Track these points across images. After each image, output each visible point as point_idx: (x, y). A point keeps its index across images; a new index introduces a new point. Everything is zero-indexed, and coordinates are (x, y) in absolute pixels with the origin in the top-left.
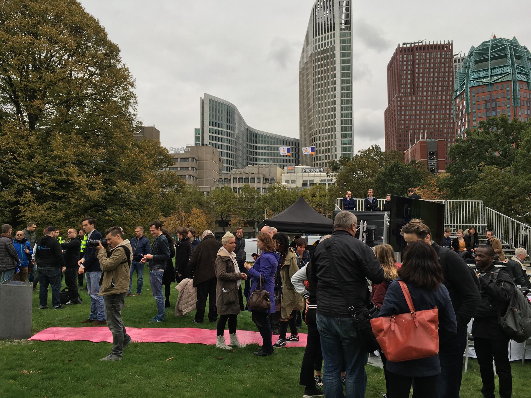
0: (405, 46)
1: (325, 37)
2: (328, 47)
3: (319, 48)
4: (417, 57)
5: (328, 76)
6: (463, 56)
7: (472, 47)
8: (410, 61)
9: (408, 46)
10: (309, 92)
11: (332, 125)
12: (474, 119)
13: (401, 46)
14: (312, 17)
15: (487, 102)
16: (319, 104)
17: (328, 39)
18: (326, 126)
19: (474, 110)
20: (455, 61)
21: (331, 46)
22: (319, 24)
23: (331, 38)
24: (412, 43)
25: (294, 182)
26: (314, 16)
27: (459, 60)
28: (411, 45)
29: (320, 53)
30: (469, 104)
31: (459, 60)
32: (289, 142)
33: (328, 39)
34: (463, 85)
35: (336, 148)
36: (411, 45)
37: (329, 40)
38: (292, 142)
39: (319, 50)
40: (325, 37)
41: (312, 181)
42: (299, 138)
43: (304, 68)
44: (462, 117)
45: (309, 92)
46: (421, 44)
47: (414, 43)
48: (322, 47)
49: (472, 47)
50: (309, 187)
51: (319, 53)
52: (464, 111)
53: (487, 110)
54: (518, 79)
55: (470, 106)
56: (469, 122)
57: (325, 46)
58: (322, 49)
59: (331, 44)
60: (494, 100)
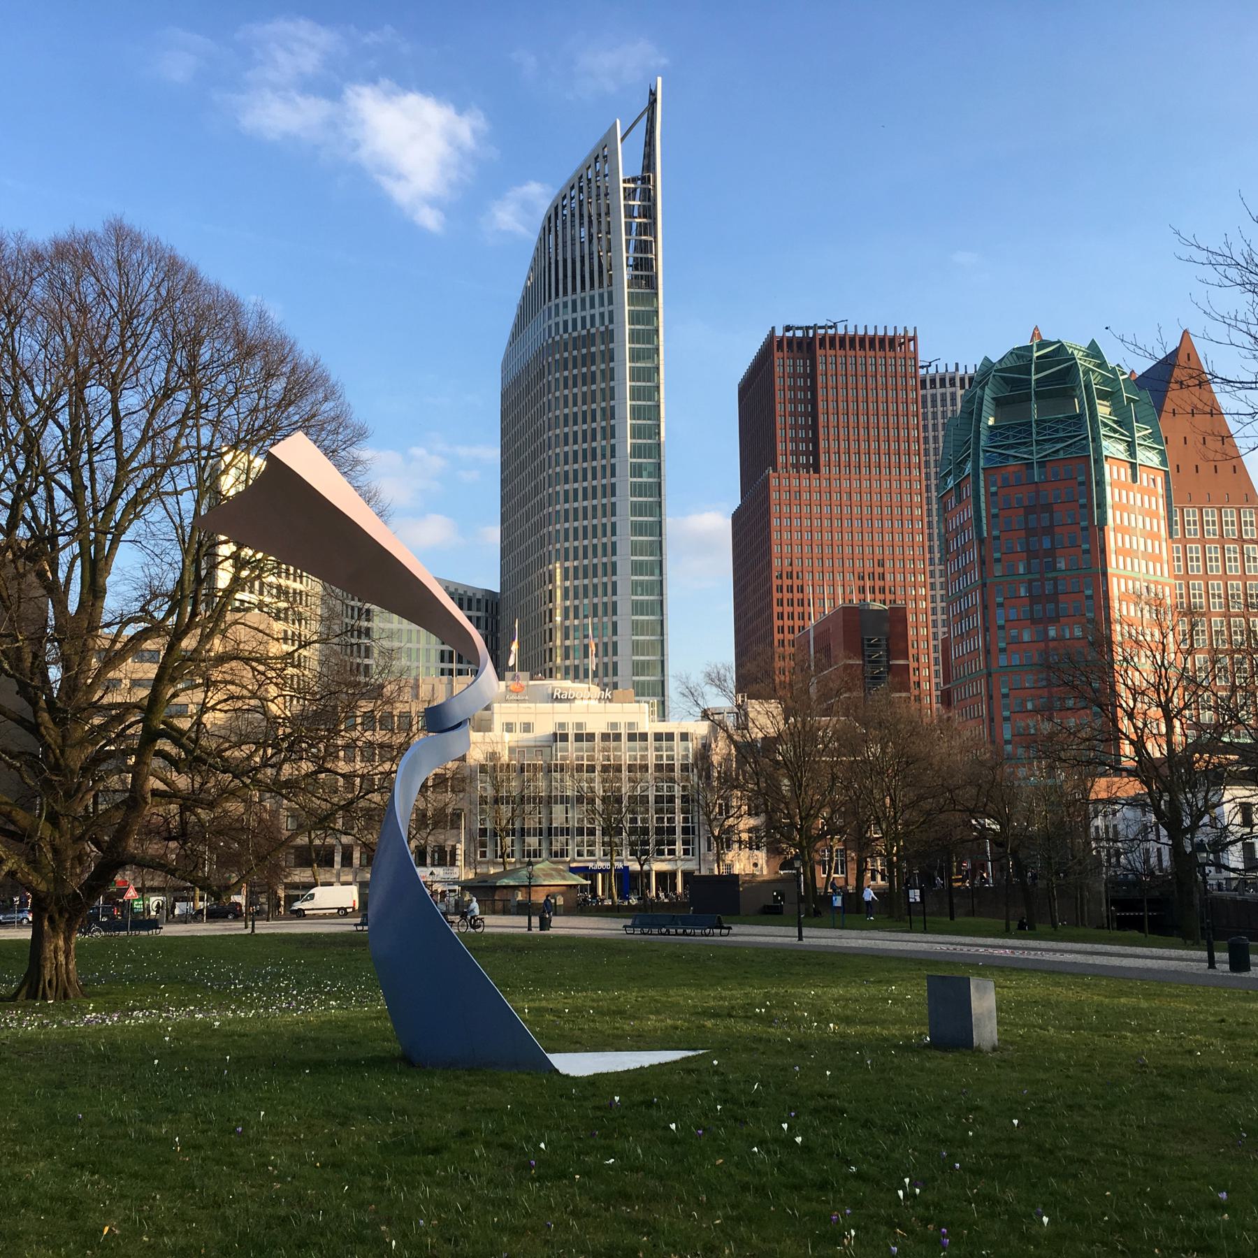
0: (790, 334)
1: (583, 300)
2: (593, 331)
3: (566, 331)
4: (821, 368)
5: (594, 411)
6: (942, 370)
7: (986, 359)
8: (804, 376)
9: (799, 334)
10: (534, 455)
11: (605, 555)
12: (997, 555)
13: (779, 333)
14: (543, 239)
15: (1029, 510)
16: (566, 492)
17: (592, 306)
18: (585, 557)
19: (996, 533)
20: (923, 382)
21: (602, 329)
22: (565, 261)
23: (602, 304)
24: (808, 328)
25: (527, 727)
26: (552, 237)
27: (933, 381)
29: (570, 347)
30: (984, 513)
31: (933, 381)
32: (470, 600)
33: (592, 306)
34: (965, 461)
35: (615, 625)
37: (597, 311)
38: (479, 601)
39: (566, 336)
40: (583, 300)
41: (579, 725)
42: (496, 589)
43: (517, 382)
44: (964, 550)
45: (534, 455)
46: (831, 332)
47: (815, 327)
48: (575, 328)
49: (986, 359)
50: (571, 744)
51: (566, 344)
52: (970, 534)
53: (1030, 532)
54: (1105, 453)
55: (984, 521)
56: (982, 562)
57: (584, 327)
58: (575, 334)
59: (603, 324)
60: (1048, 508)
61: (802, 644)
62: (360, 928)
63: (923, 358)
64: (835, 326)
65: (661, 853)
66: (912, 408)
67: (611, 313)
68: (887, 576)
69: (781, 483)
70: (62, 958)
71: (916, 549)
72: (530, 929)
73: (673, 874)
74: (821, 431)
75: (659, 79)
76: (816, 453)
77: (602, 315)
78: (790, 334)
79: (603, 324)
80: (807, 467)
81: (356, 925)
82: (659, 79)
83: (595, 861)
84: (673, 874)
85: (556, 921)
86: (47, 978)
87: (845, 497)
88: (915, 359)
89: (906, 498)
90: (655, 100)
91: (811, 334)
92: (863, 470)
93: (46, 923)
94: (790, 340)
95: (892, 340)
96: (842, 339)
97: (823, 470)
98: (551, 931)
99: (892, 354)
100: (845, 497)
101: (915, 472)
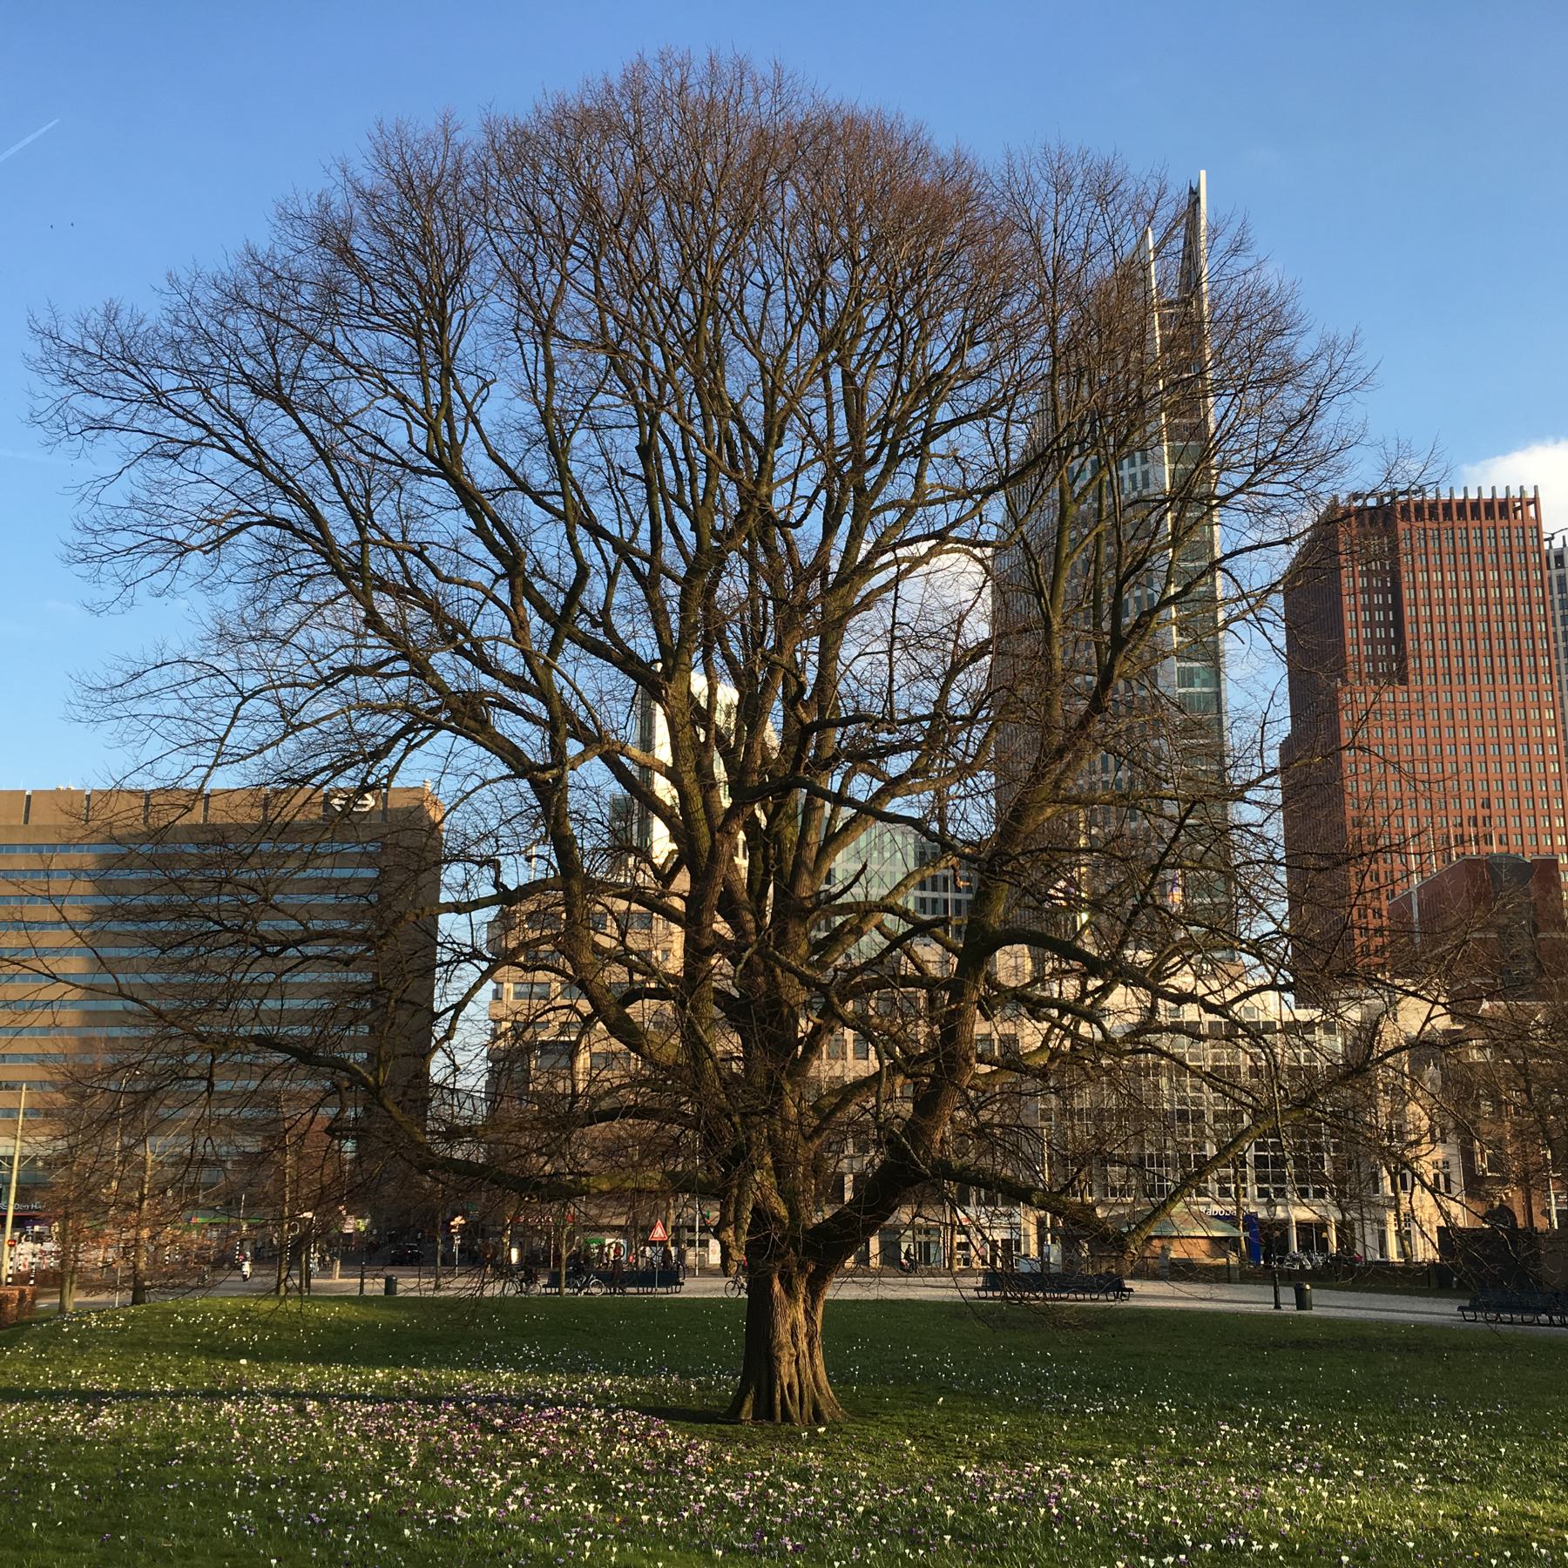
0: (1359, 503)
9: (1372, 502)
28: (1381, 500)
36: (1381, 500)
61: (1400, 912)
62: (983, 1294)
63: (1547, 528)
64: (1421, 489)
65: (1304, 1193)
66: (1537, 593)
67: (1145, 474)
68: (1496, 821)
69: (1355, 698)
70: (803, 1345)
71: (1551, 783)
72: (1277, 1307)
73: (1322, 1226)
74: (1408, 628)
75: (1203, 173)
76: (1402, 659)
77: (1133, 477)
78: (1359, 503)
79: (1135, 488)
80: (1389, 675)
81: (977, 1289)
82: (1203, 173)
83: (1208, 1204)
84: (1322, 1226)
85: (1316, 1295)
86: (786, 1381)
87: (1444, 714)
88: (1538, 528)
89: (1533, 714)
90: (1198, 200)
91: (1387, 500)
92: (1469, 678)
93: (777, 1287)
94: (1360, 511)
95: (1504, 505)
96: (1433, 506)
97: (1411, 677)
98: (1315, 1312)
99: (1505, 522)
100: (1444, 714)
101: (1544, 679)
